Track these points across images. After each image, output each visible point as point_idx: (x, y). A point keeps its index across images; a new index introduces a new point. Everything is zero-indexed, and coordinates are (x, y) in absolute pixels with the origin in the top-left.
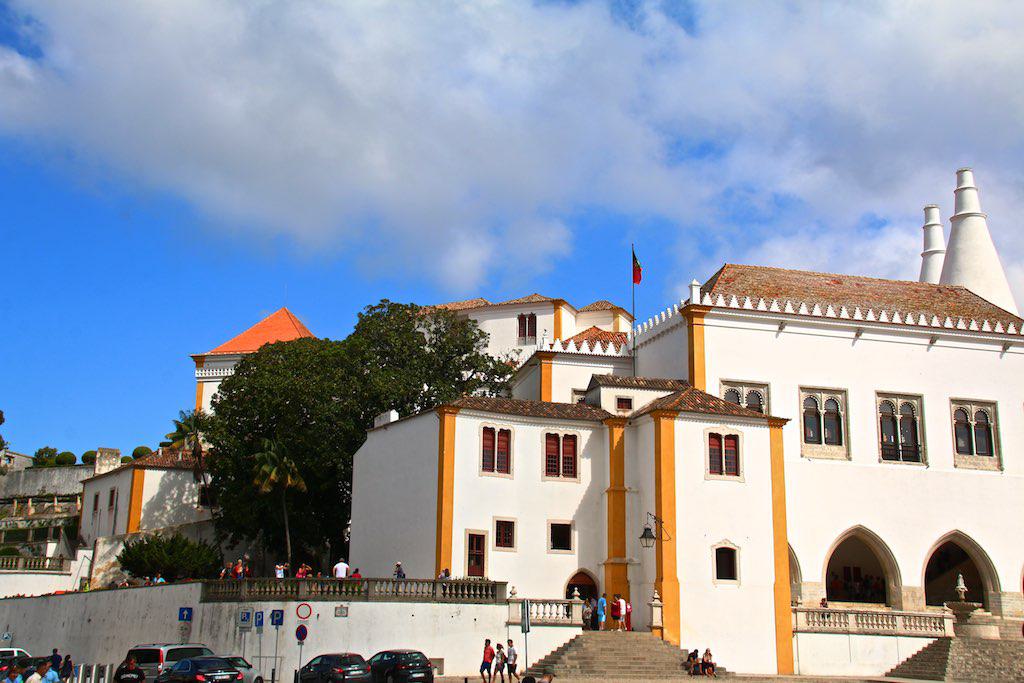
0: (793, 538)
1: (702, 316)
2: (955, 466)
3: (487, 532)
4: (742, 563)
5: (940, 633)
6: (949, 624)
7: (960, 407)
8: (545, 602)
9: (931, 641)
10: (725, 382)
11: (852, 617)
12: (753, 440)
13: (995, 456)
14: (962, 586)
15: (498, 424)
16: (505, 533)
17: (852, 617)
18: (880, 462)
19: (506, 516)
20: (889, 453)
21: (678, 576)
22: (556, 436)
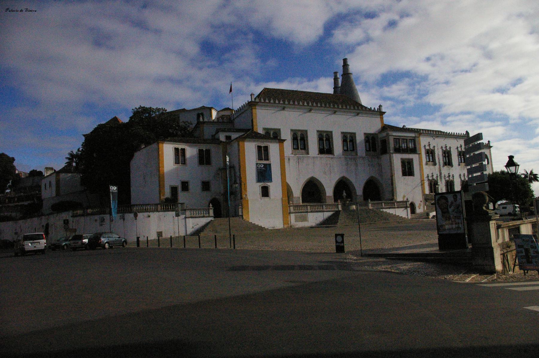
0: (288, 181)
5: (337, 209)
6: (340, 206)
10: (264, 129)
11: (309, 207)
15: (180, 146)
17: (309, 207)
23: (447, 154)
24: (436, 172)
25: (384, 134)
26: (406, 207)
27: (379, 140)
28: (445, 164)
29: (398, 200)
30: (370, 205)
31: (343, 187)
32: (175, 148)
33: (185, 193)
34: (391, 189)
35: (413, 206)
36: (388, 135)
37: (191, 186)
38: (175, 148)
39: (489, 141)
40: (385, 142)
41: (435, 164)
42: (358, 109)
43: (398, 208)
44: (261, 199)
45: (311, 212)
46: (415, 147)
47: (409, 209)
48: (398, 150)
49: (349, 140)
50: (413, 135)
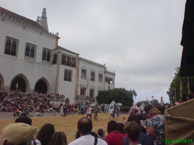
2: (24, 58)
13: (34, 58)
14: (17, 86)
18: (4, 54)
20: (7, 52)
23: (93, 74)
24: (85, 84)
25: (56, 51)
27: (53, 55)
28: (91, 79)
34: (54, 88)
35: (67, 101)
39: (114, 72)
40: (55, 56)
41: (86, 79)
42: (41, 30)
48: (63, 63)
50: (75, 56)
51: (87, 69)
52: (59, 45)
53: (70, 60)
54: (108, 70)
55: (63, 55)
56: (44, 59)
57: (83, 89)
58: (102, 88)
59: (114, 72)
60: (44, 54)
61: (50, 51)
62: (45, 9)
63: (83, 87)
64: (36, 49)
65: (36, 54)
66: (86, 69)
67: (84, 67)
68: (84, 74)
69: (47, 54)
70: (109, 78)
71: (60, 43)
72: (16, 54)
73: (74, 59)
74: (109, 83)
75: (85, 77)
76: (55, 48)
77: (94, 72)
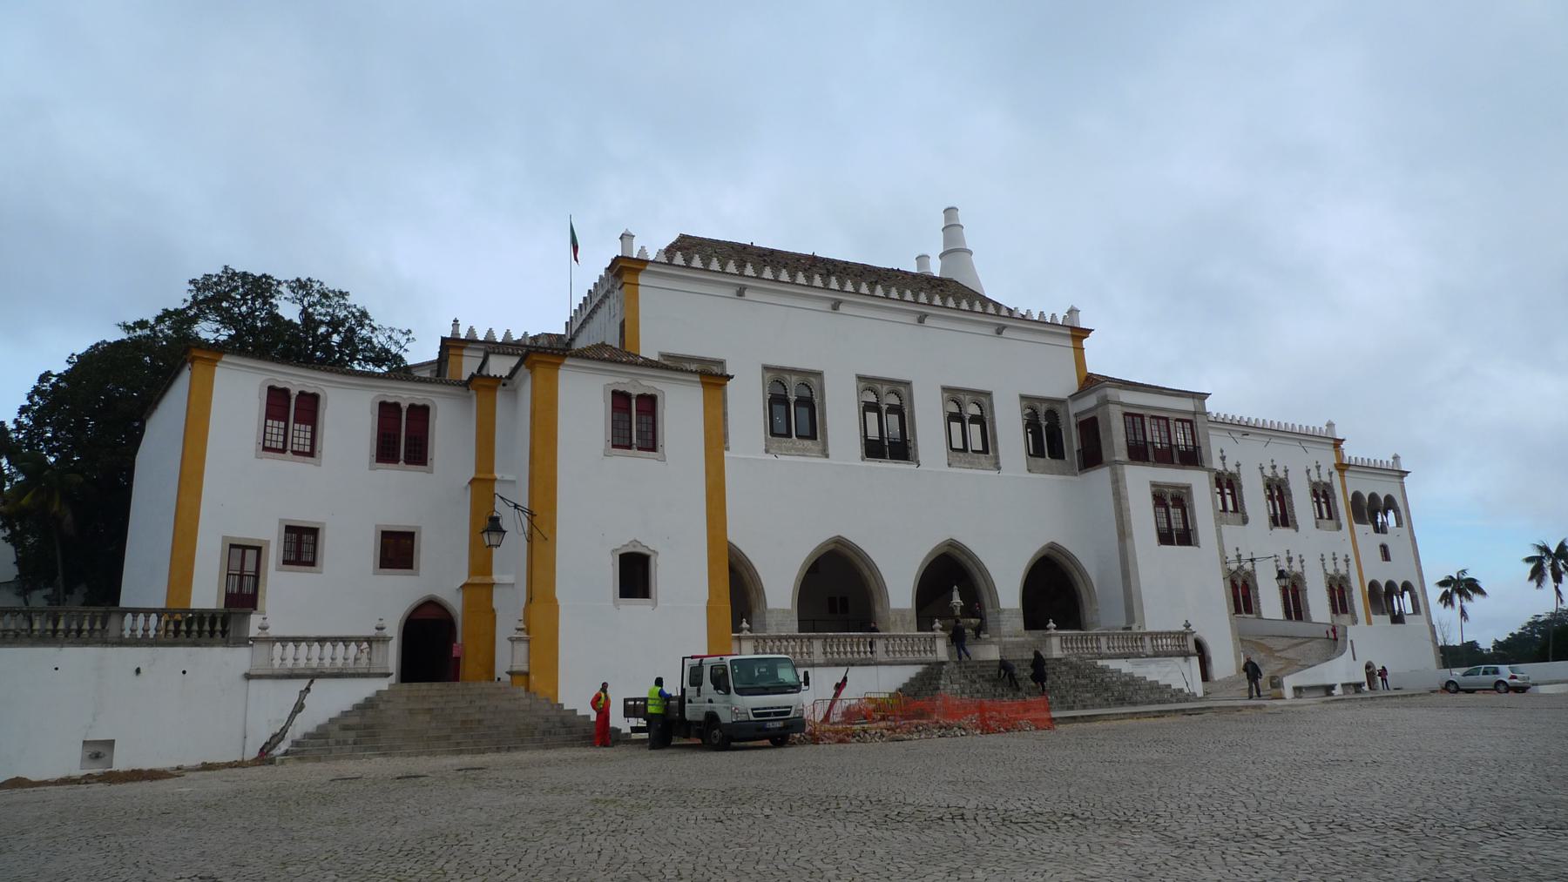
1: (637, 271)
3: (268, 543)
4: (662, 575)
5: (930, 657)
7: (953, 394)
8: (322, 640)
9: (919, 669)
12: (681, 408)
14: (957, 600)
15: (296, 380)
16: (302, 545)
17: (817, 646)
19: (303, 516)
20: (873, 449)
21: (558, 595)
22: (396, 406)
23: (1277, 491)
25: (1090, 401)
26: (1186, 655)
27: (1073, 421)
29: (1150, 627)
30: (1055, 642)
31: (950, 579)
32: (271, 389)
33: (299, 578)
35: (1201, 649)
36: (1105, 402)
37: (329, 546)
38: (271, 389)
39: (1396, 458)
40: (1090, 429)
43: (1156, 655)
44: (616, 605)
45: (827, 664)
46: (1196, 448)
47: (1195, 661)
48: (1139, 453)
49: (969, 413)
50: (1187, 405)
51: (1238, 465)
52: (1093, 367)
53: (1167, 435)
54: (1351, 452)
55: (1126, 414)
56: (1036, 452)
57: (1240, 583)
58: (1347, 561)
59: (1396, 458)
60: (1032, 424)
61: (1057, 406)
62: (950, 212)
63: (1240, 568)
64: (992, 412)
65: (994, 437)
66: (1234, 470)
67: (1223, 458)
68: (1229, 498)
69: (1044, 423)
70: (1373, 497)
71: (1099, 360)
72: (911, 452)
73: (1189, 422)
74: (1381, 529)
75: (1236, 510)
76: (1073, 386)
77: (1281, 475)
